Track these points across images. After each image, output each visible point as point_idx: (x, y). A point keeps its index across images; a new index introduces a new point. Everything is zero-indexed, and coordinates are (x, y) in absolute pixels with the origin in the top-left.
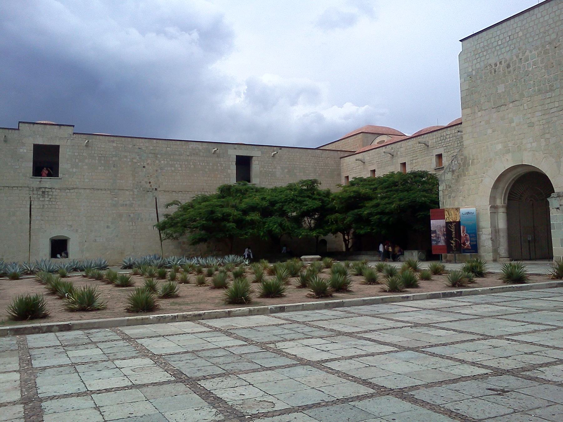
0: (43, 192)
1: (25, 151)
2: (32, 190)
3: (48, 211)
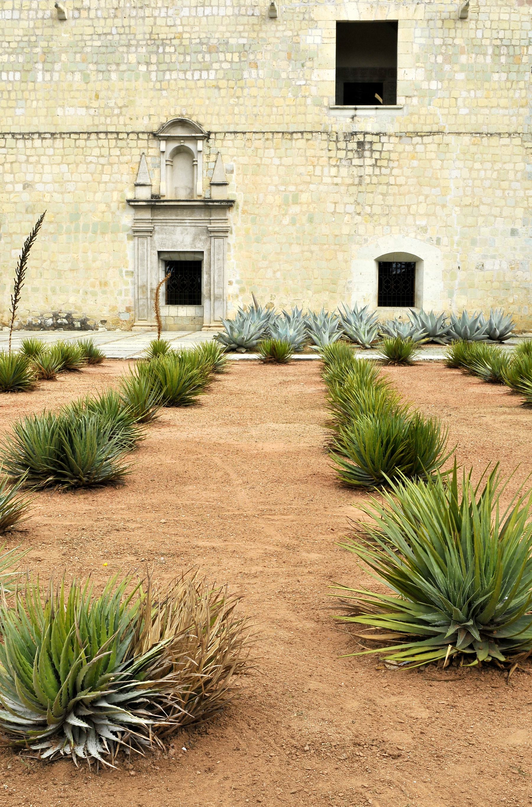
0: (361, 144)
1: (318, 40)
2: (335, 139)
3: (372, 192)
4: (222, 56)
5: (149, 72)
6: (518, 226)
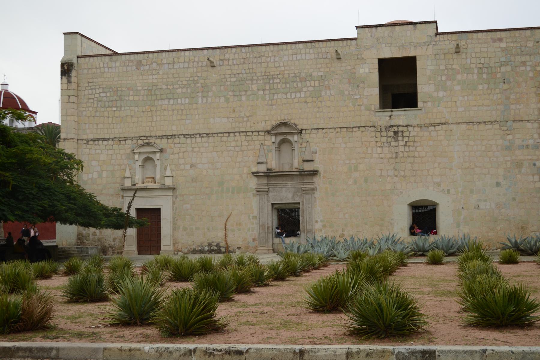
0: (396, 133)
1: (367, 71)
2: (379, 130)
3: (404, 162)
4: (308, 83)
5: (265, 95)
6: (500, 180)
